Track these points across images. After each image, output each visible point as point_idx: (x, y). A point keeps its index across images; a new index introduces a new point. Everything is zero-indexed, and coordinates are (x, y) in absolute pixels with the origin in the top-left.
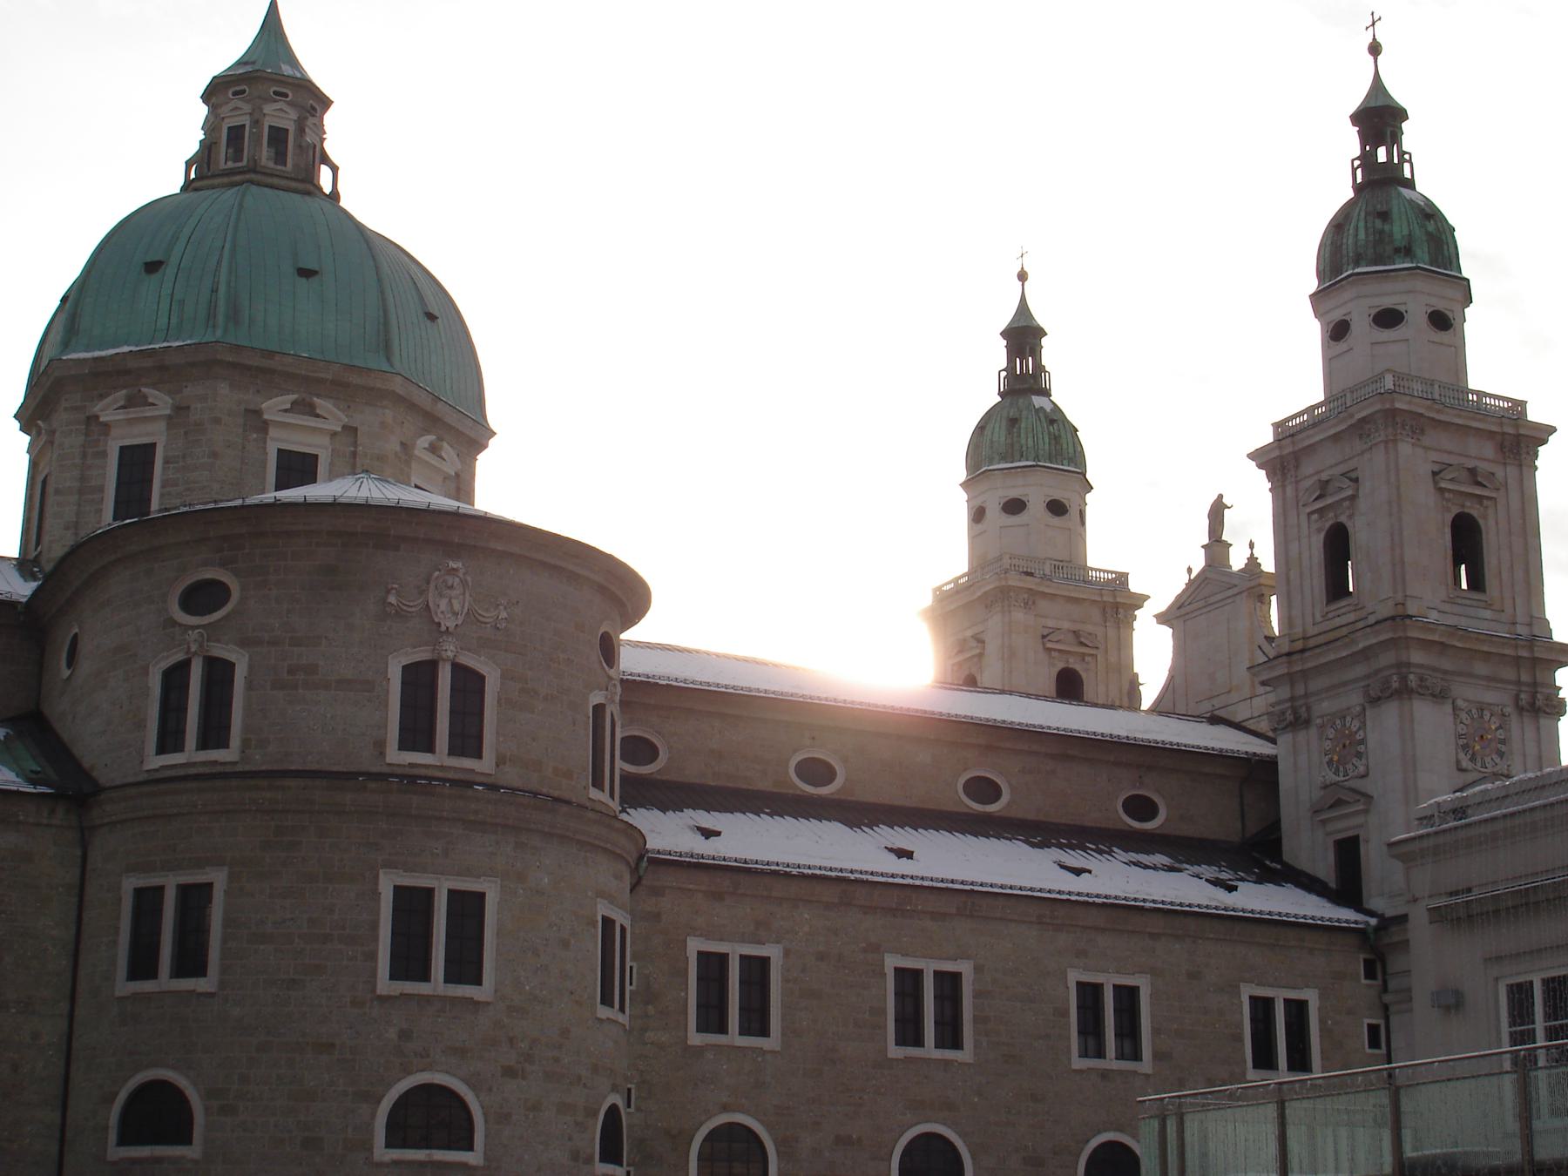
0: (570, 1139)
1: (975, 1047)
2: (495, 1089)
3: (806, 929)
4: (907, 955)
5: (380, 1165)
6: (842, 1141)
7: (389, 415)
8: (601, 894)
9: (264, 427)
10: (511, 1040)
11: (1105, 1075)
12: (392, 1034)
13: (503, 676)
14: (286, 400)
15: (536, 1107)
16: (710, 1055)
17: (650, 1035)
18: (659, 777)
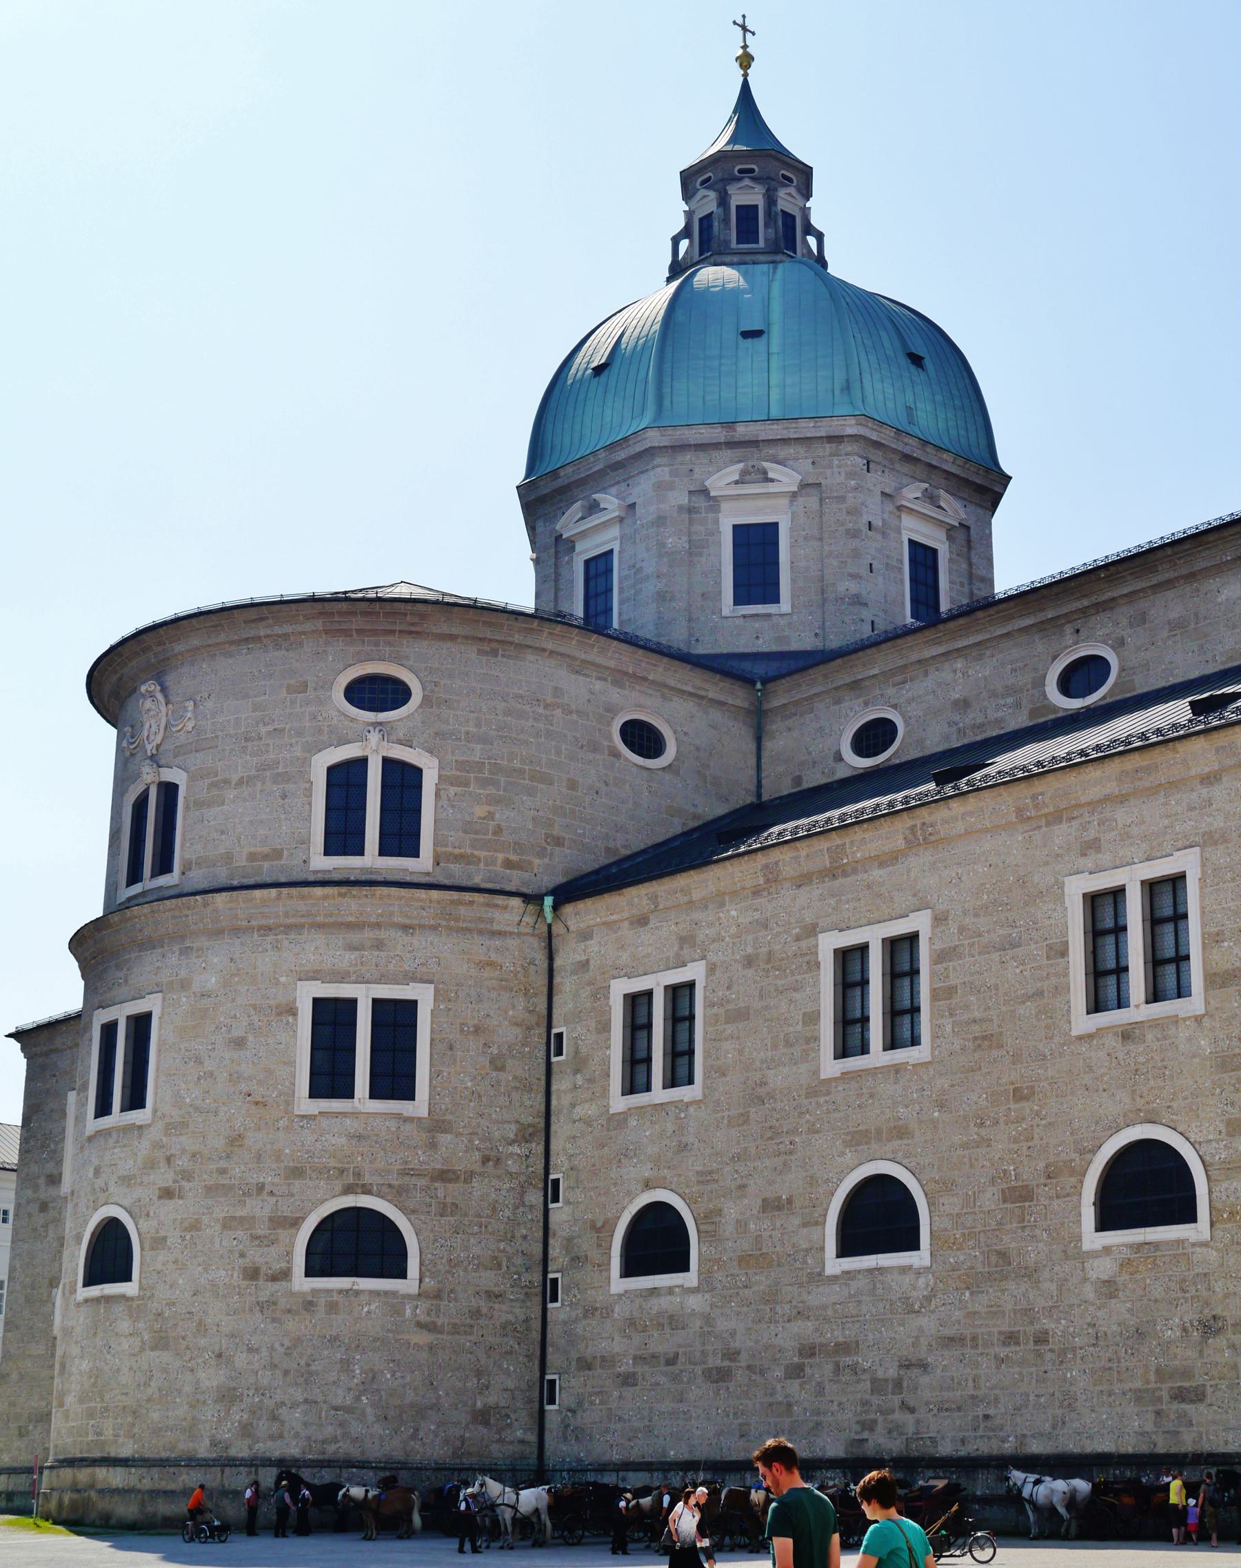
0: (242, 1255)
1: (935, 1037)
2: (152, 1214)
3: (733, 930)
4: (848, 928)
5: (78, 1305)
6: (772, 1206)
7: (661, 471)
8: (314, 976)
9: (570, 545)
10: (169, 1160)
11: (1127, 1034)
12: (91, 1175)
13: (193, 778)
14: (576, 509)
15: (195, 1226)
16: (633, 1122)
17: (579, 1111)
18: (897, 761)
